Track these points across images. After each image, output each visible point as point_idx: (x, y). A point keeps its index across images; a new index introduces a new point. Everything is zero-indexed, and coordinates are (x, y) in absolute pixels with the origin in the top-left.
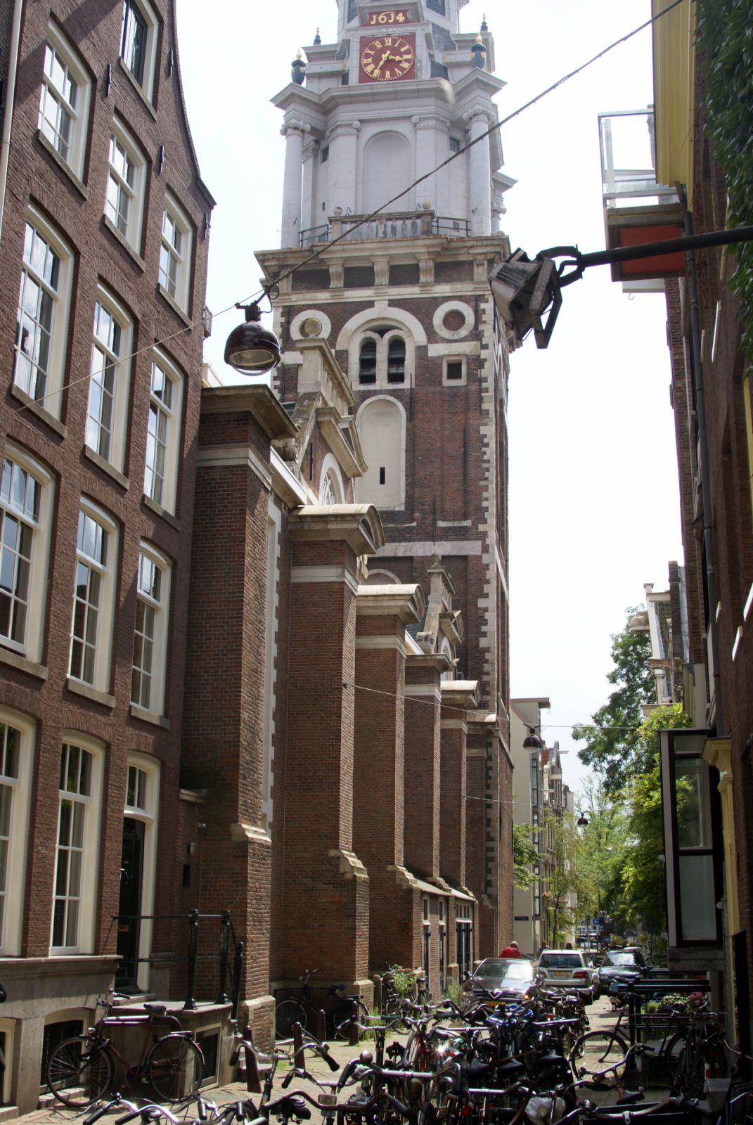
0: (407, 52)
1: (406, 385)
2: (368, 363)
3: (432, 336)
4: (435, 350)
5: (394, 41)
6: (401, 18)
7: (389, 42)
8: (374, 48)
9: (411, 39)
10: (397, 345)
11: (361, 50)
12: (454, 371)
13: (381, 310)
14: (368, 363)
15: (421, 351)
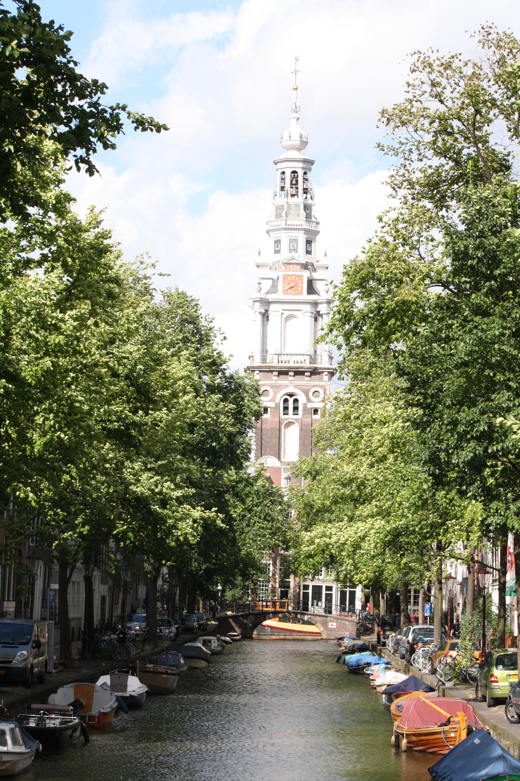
0: (300, 283)
1: (299, 416)
2: (286, 408)
3: (309, 400)
4: (309, 406)
5: (295, 278)
6: (298, 267)
7: (293, 277)
8: (287, 280)
9: (301, 277)
10: (296, 401)
11: (283, 281)
12: (316, 411)
13: (291, 390)
14: (286, 408)
15: (305, 405)
